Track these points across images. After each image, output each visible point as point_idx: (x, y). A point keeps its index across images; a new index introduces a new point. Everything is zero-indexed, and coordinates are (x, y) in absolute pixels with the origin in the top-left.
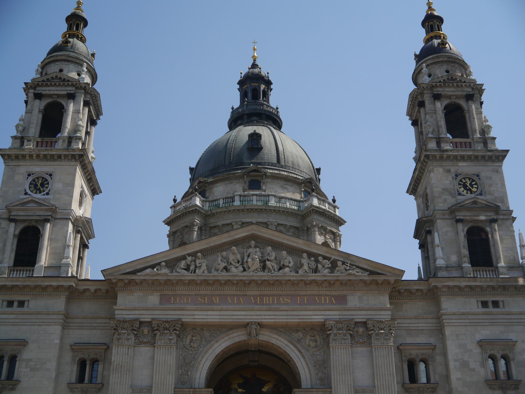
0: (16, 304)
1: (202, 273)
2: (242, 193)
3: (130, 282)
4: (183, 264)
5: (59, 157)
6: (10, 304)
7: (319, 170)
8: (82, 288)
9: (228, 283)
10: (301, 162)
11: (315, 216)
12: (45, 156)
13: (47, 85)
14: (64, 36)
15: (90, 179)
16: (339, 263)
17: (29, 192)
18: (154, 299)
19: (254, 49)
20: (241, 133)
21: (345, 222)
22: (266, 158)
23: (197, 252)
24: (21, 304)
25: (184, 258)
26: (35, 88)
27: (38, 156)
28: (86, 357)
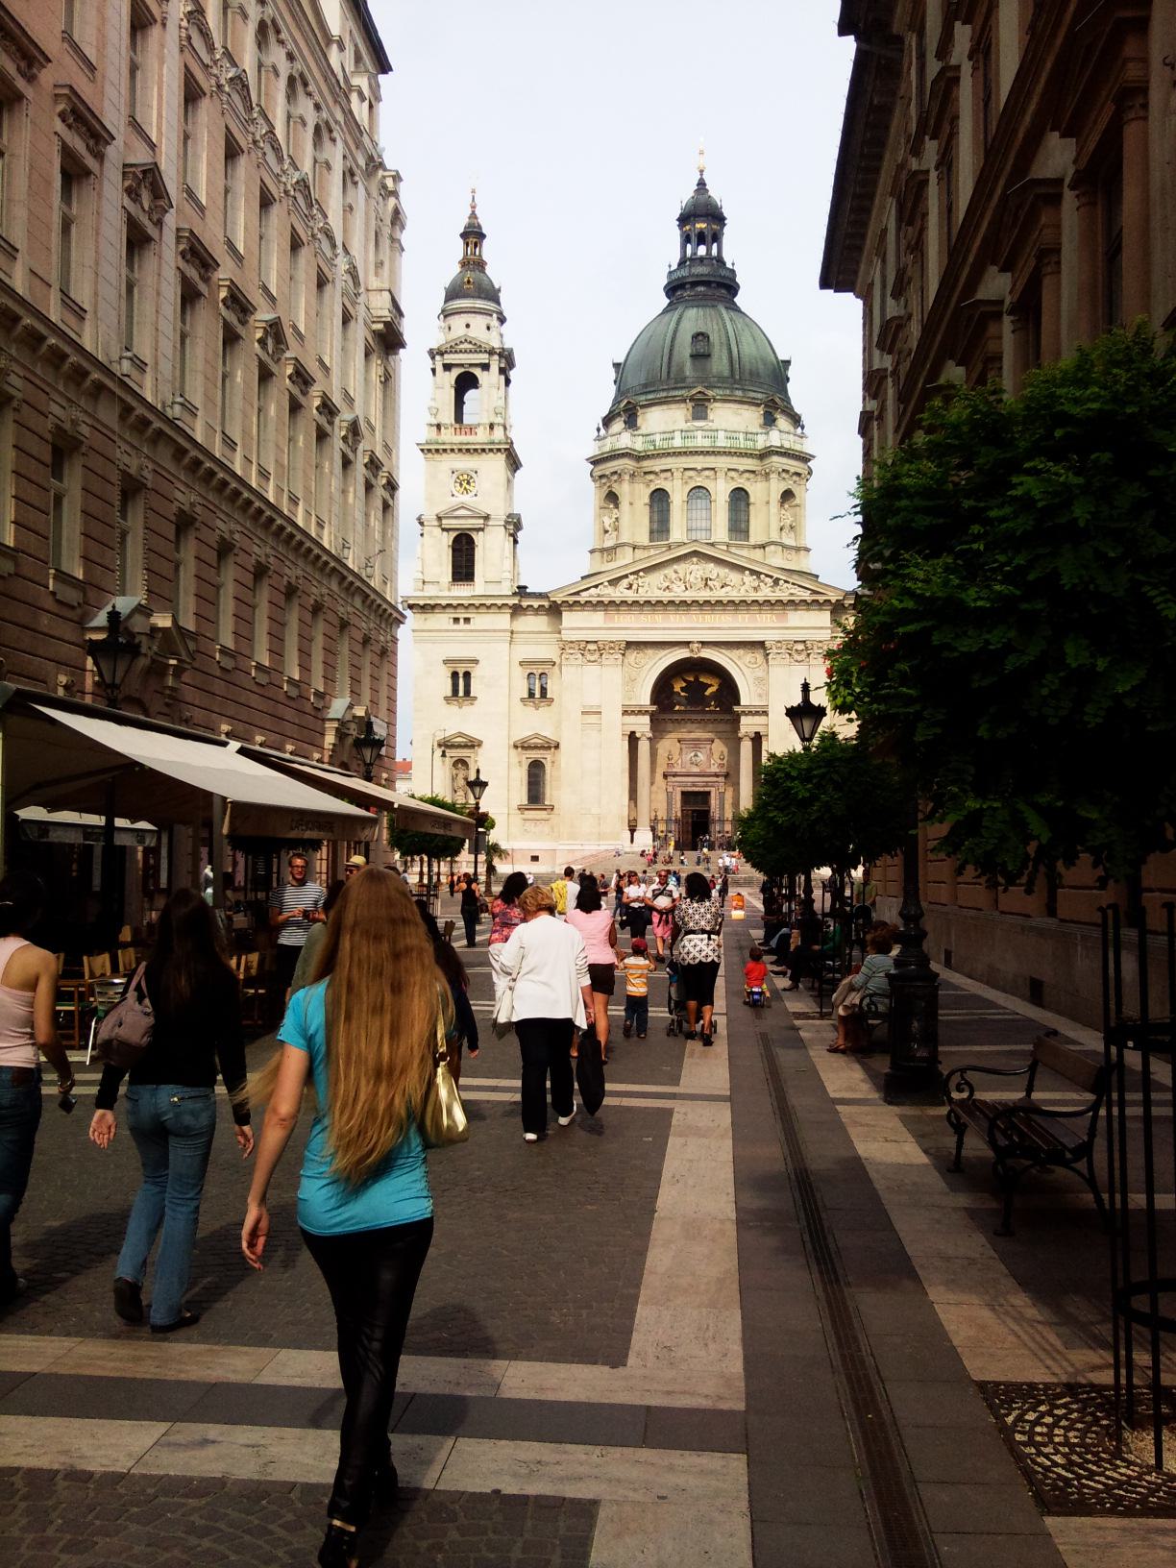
0: (462, 621)
1: (642, 595)
2: (684, 426)
3: (575, 602)
4: (625, 582)
5: (483, 450)
6: (456, 620)
7: (787, 363)
8: (525, 604)
9: (671, 602)
10: (761, 367)
11: (775, 458)
12: (468, 450)
13: (456, 352)
14: (465, 264)
15: (515, 462)
16: (781, 582)
17: (455, 493)
18: (597, 618)
19: (701, 153)
20: (682, 325)
21: (814, 457)
22: (714, 370)
23: (639, 571)
24: (467, 620)
25: (626, 576)
26: (442, 354)
27: (460, 450)
28: (535, 671)
